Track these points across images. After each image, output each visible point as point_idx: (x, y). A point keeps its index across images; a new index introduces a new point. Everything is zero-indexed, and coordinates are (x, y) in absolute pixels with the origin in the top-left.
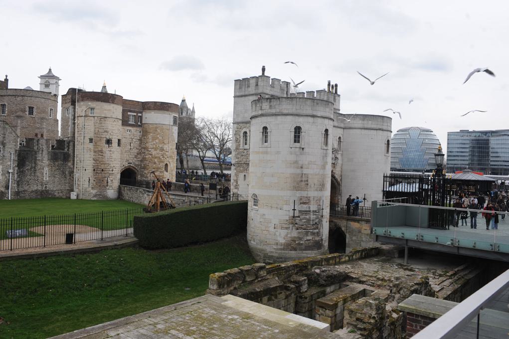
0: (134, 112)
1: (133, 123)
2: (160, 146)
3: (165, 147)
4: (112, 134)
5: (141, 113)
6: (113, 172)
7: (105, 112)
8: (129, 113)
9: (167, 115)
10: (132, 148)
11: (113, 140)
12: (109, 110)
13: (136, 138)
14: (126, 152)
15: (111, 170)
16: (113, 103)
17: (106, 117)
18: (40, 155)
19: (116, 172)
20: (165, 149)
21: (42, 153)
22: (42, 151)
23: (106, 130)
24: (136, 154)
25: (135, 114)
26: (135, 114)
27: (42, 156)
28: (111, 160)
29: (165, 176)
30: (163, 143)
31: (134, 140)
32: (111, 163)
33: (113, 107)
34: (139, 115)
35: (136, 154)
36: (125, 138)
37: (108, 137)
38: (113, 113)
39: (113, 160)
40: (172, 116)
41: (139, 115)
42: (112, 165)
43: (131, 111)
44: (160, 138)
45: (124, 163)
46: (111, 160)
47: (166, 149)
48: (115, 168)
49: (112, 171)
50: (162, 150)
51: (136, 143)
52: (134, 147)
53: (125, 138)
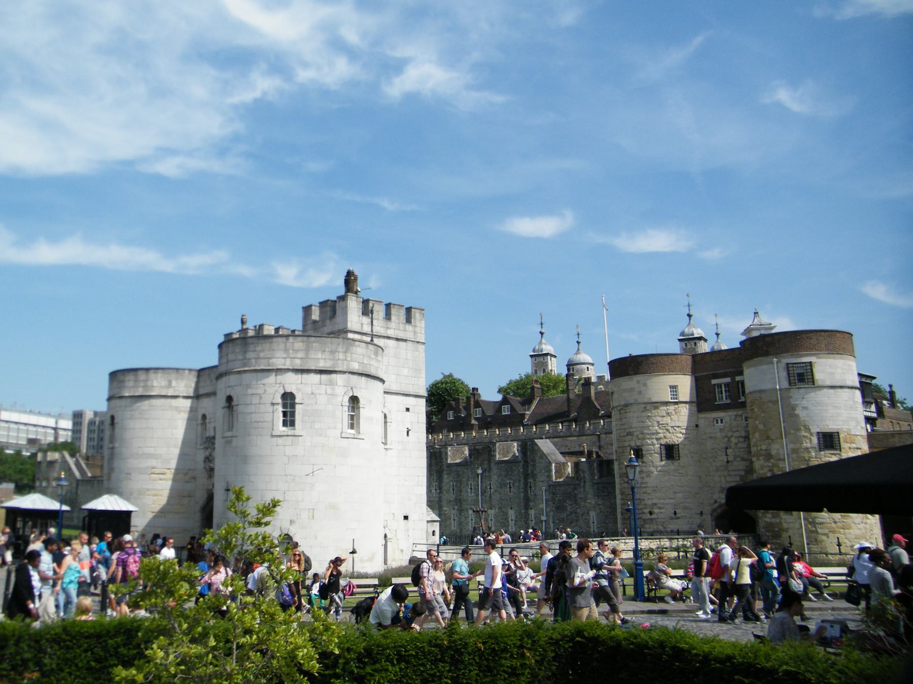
0: (724, 375)
1: (725, 401)
2: (764, 447)
3: (774, 449)
4: (640, 436)
5: (741, 373)
6: (653, 516)
7: (625, 394)
8: (714, 382)
9: (764, 367)
10: (731, 458)
11: (643, 448)
12: (632, 390)
13: (737, 434)
14: (717, 470)
15: (647, 511)
16: (636, 373)
17: (626, 405)
18: (582, 489)
19: (661, 516)
20: (773, 452)
21: (584, 486)
22: (585, 482)
23: (628, 430)
24: (743, 473)
25: (728, 380)
26: (728, 380)
27: (584, 491)
28: (644, 490)
29: (785, 526)
30: (768, 438)
31: (734, 440)
32: (646, 497)
33: (638, 382)
34: (738, 378)
35: (743, 473)
36: (711, 438)
37: (633, 444)
38: (640, 393)
39: (649, 490)
40: (782, 365)
41: (738, 378)
42: (649, 502)
43: (716, 376)
44: (761, 427)
45: (716, 496)
46: (644, 490)
47: (778, 454)
48: (660, 508)
49: (651, 513)
50: (768, 456)
51: (740, 445)
52: (735, 457)
53: (711, 438)
